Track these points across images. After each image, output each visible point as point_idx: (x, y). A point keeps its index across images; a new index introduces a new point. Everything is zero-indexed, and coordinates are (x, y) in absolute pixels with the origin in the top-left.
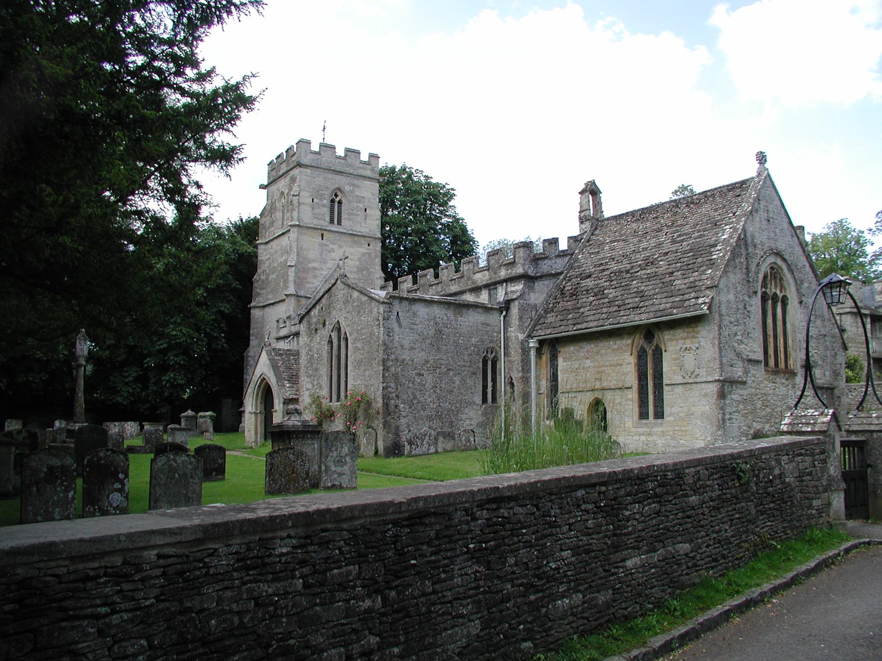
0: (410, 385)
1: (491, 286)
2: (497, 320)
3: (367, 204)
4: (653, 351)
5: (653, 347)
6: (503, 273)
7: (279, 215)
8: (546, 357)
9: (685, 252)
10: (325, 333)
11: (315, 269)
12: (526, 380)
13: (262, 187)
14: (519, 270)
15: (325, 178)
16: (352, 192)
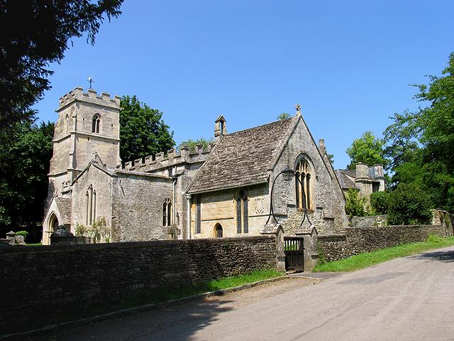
1: (170, 168)
2: (171, 185)
3: (113, 122)
6: (175, 161)
7: (65, 126)
9: (260, 153)
10: (85, 190)
11: (84, 156)
12: (184, 215)
14: (182, 160)
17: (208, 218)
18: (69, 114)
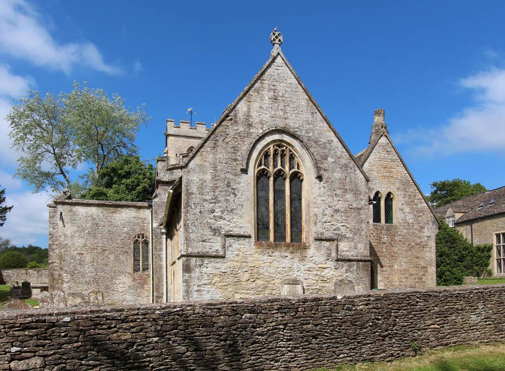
0: (72, 261)
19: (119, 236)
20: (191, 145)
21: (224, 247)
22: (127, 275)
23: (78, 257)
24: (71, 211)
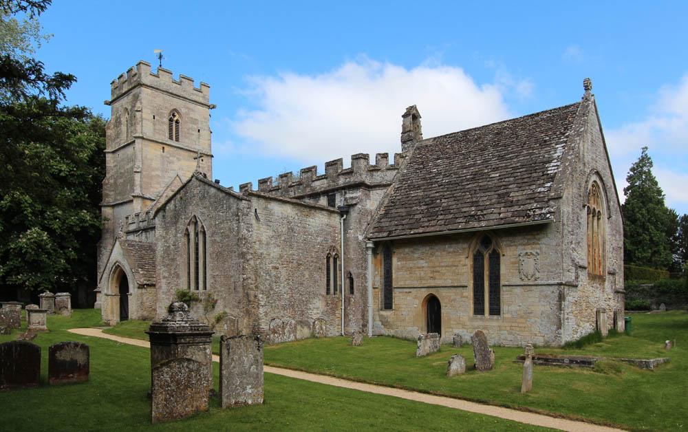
1: (330, 194)
2: (336, 220)
3: (200, 126)
4: (490, 255)
5: (490, 252)
6: (342, 181)
7: (124, 128)
8: (380, 257)
10: (181, 227)
13: (107, 103)
15: (164, 99)
16: (187, 114)
17: (408, 283)
18: (129, 108)
19: (314, 247)
20: (172, 108)
21: (577, 278)
22: (321, 297)
23: (273, 273)
24: (266, 208)
